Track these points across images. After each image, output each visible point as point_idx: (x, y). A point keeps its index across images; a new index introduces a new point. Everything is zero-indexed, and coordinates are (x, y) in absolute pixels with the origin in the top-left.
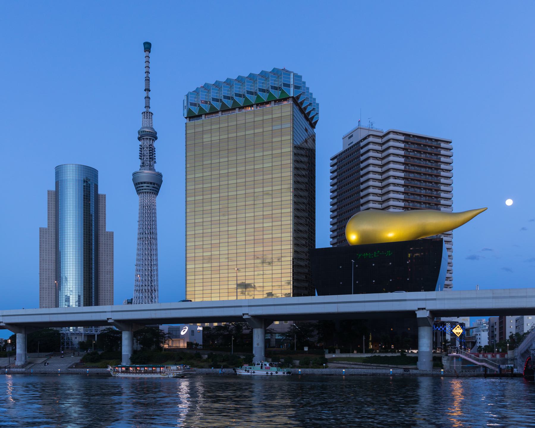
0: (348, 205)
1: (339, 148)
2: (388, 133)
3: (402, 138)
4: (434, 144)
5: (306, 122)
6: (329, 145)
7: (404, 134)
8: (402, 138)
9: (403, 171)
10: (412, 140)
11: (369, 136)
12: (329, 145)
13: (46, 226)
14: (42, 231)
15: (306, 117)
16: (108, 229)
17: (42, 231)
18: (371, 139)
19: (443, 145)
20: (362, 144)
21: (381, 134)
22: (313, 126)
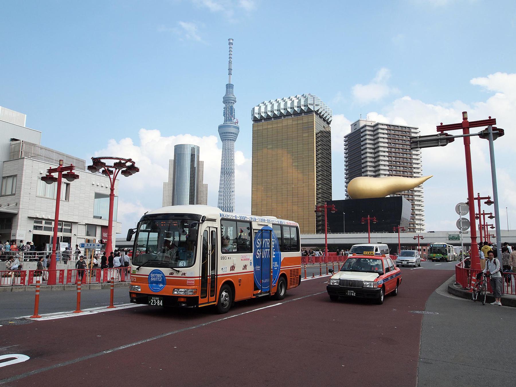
0: (355, 168)
1: (348, 131)
2: (377, 124)
3: (386, 127)
4: (407, 130)
5: (324, 122)
6: (340, 131)
7: (387, 125)
8: (386, 127)
9: (388, 147)
10: (392, 128)
11: (365, 126)
12: (340, 131)
13: (167, 181)
14: (165, 184)
15: (324, 120)
16: (204, 182)
17: (165, 184)
18: (368, 128)
19: (413, 130)
20: (362, 130)
21: (372, 125)
22: (329, 123)
